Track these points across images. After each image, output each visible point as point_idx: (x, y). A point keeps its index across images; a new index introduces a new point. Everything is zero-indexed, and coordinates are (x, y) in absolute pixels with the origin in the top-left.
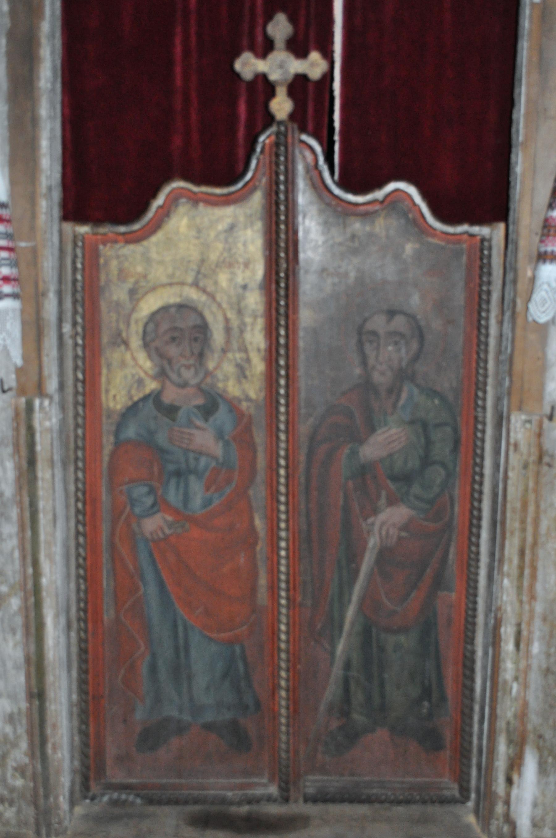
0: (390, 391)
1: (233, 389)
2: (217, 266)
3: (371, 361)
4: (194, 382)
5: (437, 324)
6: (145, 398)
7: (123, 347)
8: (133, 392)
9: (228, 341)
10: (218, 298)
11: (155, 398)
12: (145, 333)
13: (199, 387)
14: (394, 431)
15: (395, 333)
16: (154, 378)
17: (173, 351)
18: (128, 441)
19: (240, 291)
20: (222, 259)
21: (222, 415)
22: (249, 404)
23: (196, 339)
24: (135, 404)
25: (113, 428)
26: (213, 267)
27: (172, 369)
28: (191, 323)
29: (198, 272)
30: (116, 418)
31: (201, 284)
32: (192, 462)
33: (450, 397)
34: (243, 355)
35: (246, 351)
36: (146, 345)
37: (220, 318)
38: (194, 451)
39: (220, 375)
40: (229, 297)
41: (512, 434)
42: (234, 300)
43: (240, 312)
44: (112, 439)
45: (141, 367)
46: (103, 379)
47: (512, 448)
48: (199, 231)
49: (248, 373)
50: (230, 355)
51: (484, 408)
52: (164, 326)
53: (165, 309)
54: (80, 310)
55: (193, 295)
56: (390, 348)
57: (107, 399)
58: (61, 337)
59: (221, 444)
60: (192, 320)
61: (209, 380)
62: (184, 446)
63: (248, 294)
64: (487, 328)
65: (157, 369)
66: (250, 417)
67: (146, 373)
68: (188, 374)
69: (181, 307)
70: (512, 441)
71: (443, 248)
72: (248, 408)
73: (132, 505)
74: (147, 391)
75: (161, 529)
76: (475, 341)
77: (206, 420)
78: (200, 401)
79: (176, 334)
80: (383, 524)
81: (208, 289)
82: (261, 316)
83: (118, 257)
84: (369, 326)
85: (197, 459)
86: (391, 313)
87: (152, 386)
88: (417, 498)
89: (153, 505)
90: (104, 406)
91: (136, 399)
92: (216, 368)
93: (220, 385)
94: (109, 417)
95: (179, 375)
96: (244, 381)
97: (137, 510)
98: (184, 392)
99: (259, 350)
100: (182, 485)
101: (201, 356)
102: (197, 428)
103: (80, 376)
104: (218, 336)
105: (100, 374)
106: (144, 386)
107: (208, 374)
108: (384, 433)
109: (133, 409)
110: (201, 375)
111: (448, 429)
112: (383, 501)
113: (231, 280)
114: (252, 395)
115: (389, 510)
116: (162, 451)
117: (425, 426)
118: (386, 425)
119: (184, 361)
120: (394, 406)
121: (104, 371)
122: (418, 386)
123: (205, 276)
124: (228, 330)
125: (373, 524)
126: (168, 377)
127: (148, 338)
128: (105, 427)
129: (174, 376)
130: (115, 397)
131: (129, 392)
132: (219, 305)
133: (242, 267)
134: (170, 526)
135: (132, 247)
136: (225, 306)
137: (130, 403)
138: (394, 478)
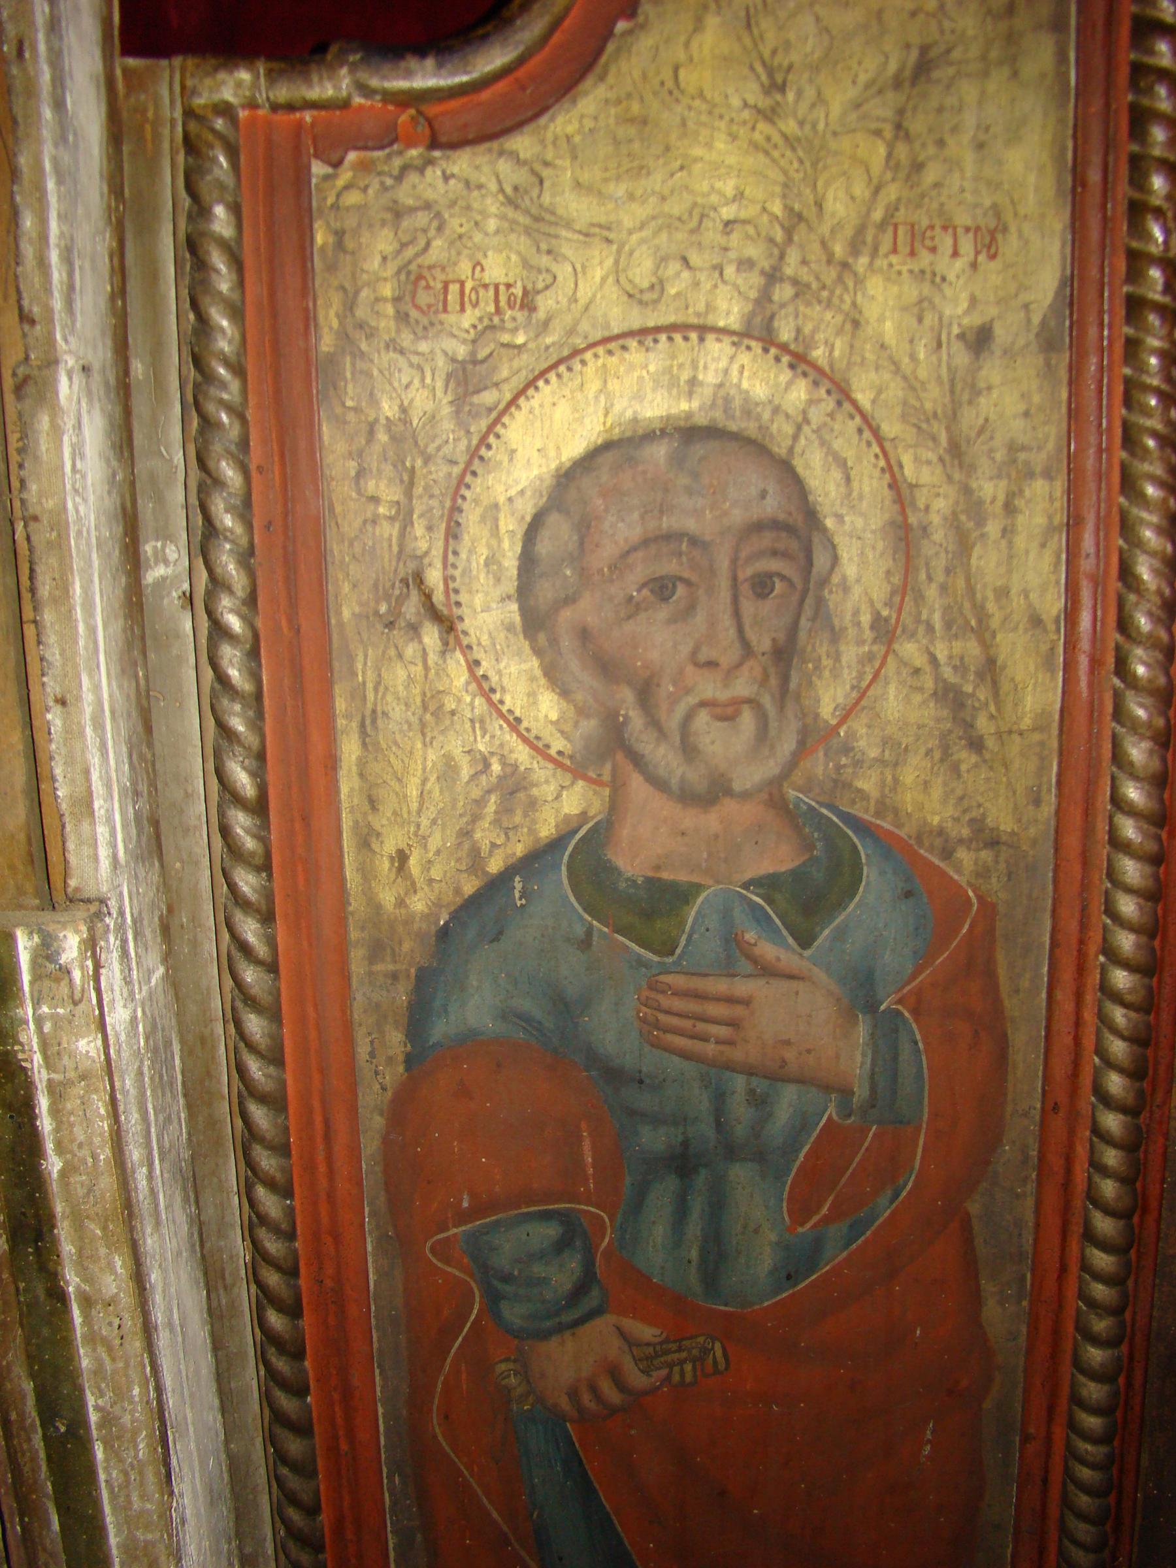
1: (924, 798)
2: (855, 247)
4: (752, 775)
6: (538, 859)
7: (431, 636)
8: (484, 835)
9: (905, 589)
10: (864, 398)
11: (583, 854)
12: (528, 560)
13: (773, 797)
16: (575, 767)
17: (659, 641)
18: (469, 1044)
19: (962, 358)
20: (878, 215)
21: (874, 915)
22: (986, 855)
23: (762, 586)
24: (498, 885)
25: (402, 995)
26: (838, 249)
27: (655, 723)
28: (738, 516)
29: (772, 277)
30: (411, 951)
31: (785, 334)
32: (740, 1111)
34: (972, 649)
35: (983, 632)
36: (535, 623)
37: (870, 482)
38: (750, 1071)
39: (867, 745)
40: (912, 385)
42: (934, 397)
43: (956, 451)
44: (396, 1039)
45: (515, 724)
46: (348, 785)
48: (775, 86)
49: (983, 724)
50: (909, 649)
52: (622, 529)
53: (617, 450)
54: (229, 472)
55: (757, 380)
57: (367, 873)
58: (135, 603)
59: (862, 1031)
60: (749, 494)
61: (819, 765)
62: (710, 1049)
63: (992, 371)
65: (590, 725)
66: (988, 909)
67: (539, 748)
68: (724, 744)
69: (688, 434)
72: (983, 873)
73: (493, 1298)
74: (546, 830)
75: (614, 1373)
77: (805, 941)
78: (778, 857)
79: (670, 567)
81: (818, 354)
82: (1048, 475)
83: (398, 213)
85: (760, 1102)
87: (564, 802)
89: (580, 1290)
90: (356, 904)
91: (495, 866)
92: (847, 714)
93: (868, 783)
94: (377, 950)
95: (689, 750)
96: (967, 759)
97: (514, 1313)
98: (711, 821)
99: (1036, 621)
100: (697, 1206)
101: (785, 654)
102: (767, 971)
103: (243, 780)
104: (860, 568)
105: (332, 763)
106: (532, 805)
107: (814, 735)
109: (484, 909)
110: (787, 745)
113: (920, 309)
114: (1002, 819)
116: (614, 1075)
119: (709, 687)
121: (350, 749)
123: (801, 289)
124: (904, 536)
126: (637, 760)
127: (546, 591)
128: (360, 996)
129: (664, 756)
130: (402, 857)
131: (465, 834)
132: (869, 426)
133: (967, 246)
134: (647, 1363)
135: (462, 163)
136: (890, 429)
137: (470, 887)
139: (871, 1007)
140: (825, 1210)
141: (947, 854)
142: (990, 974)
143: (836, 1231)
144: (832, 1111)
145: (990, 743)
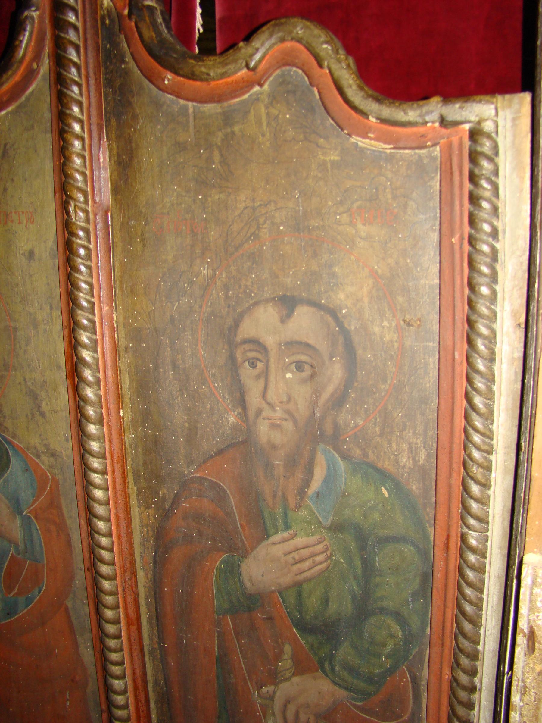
0: (291, 463)
3: (254, 399)
5: (383, 329)
14: (301, 540)
15: (292, 345)
33: (415, 487)
41: (523, 609)
47: (521, 640)
49: (45, 407)
51: (484, 520)
56: (289, 375)
59: (18, 521)
64: (491, 340)
70: (523, 624)
71: (390, 158)
76: (462, 368)
80: (288, 702)
84: (247, 329)
86: (288, 304)
88: (351, 670)
108: (284, 540)
111: (408, 550)
112: (286, 663)
115: (296, 679)
117: (362, 538)
118: (287, 527)
120: (301, 493)
122: (345, 457)
125: (272, 698)
138: (305, 628)
139: (20, 513)
140: (16, 590)
141: (38, 457)
142: (59, 507)
143: (21, 600)
144: (12, 551)
145: (47, 414)
